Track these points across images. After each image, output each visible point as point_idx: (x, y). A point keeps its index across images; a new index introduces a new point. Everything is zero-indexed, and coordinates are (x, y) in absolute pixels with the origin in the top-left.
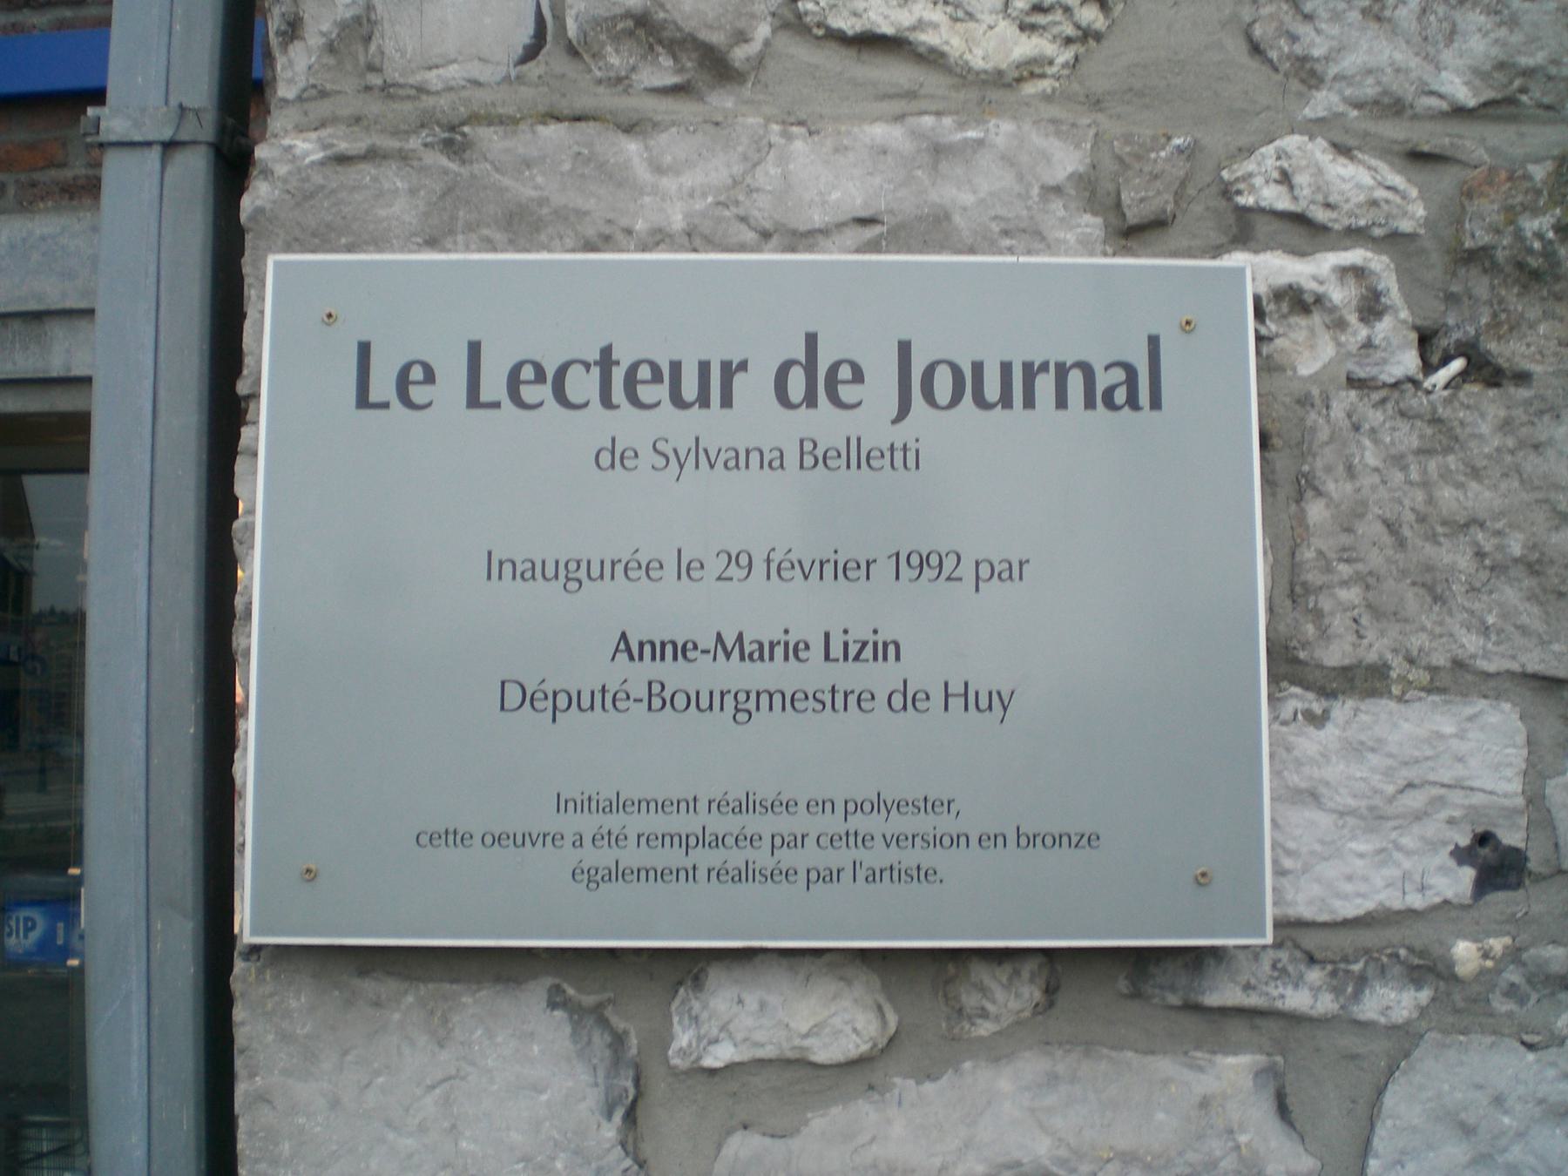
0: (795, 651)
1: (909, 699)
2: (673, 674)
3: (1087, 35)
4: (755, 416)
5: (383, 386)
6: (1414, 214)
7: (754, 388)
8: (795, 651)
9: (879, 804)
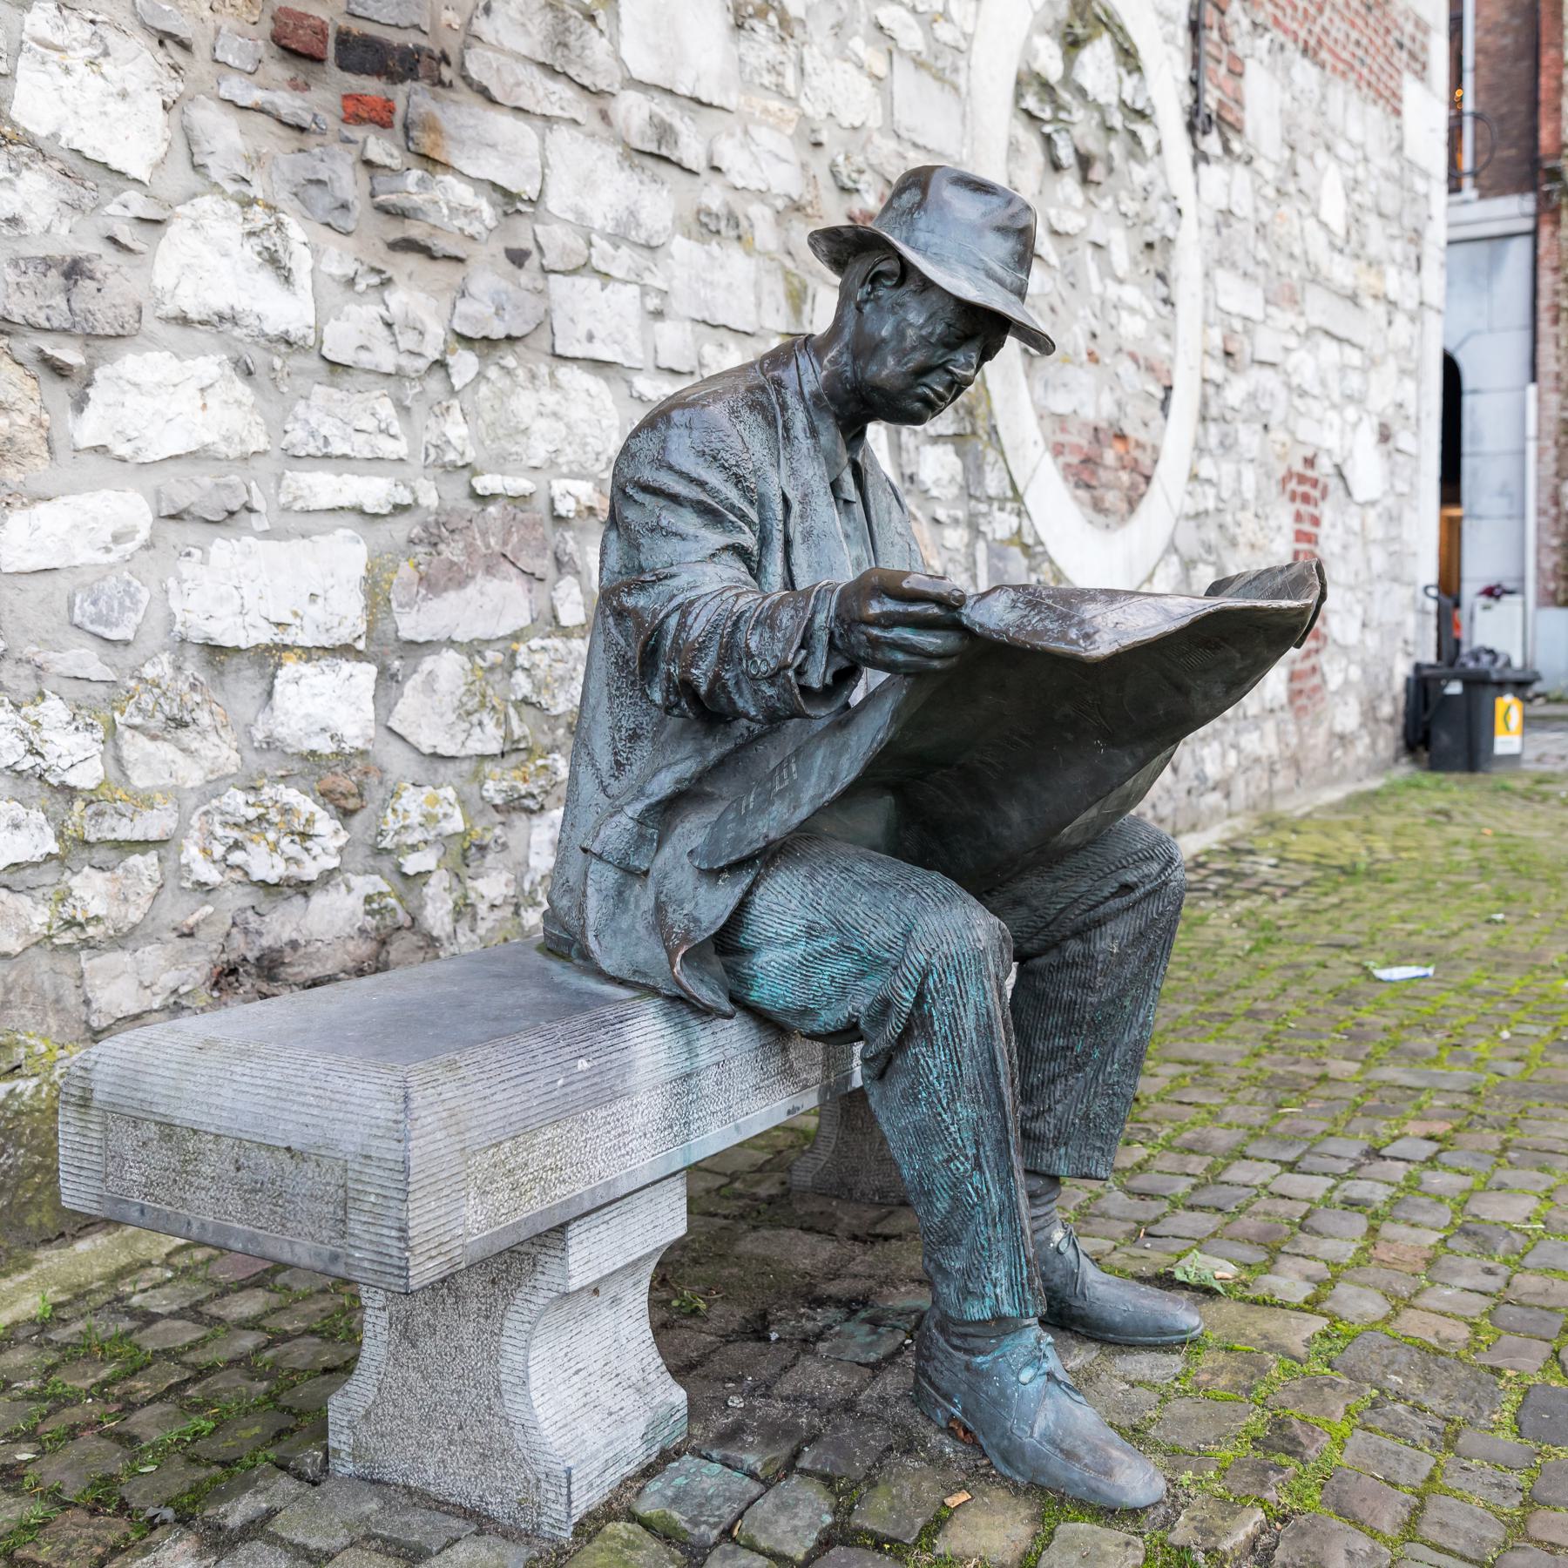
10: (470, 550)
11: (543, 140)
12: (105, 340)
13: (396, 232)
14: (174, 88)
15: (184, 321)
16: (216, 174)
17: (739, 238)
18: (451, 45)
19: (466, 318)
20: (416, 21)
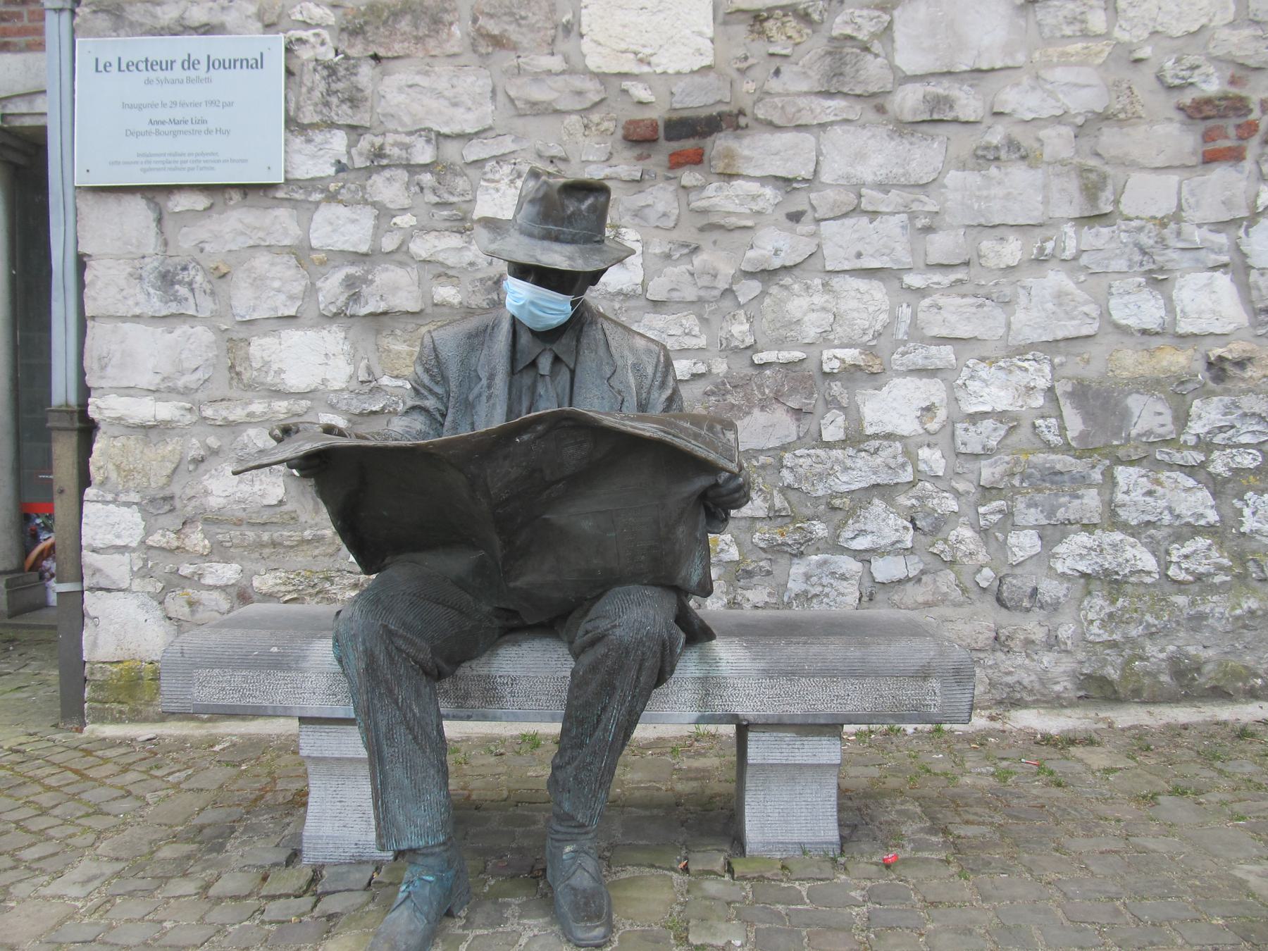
0: (186, 122)
1: (209, 132)
2: (161, 128)
4: (177, 72)
5: (101, 67)
6: (332, 20)
7: (177, 66)
8: (186, 122)
9: (202, 154)
10: (748, 398)
11: (818, 139)
13: (703, 221)
17: (1023, 158)
18: (746, 104)
19: (749, 260)
20: (718, 98)
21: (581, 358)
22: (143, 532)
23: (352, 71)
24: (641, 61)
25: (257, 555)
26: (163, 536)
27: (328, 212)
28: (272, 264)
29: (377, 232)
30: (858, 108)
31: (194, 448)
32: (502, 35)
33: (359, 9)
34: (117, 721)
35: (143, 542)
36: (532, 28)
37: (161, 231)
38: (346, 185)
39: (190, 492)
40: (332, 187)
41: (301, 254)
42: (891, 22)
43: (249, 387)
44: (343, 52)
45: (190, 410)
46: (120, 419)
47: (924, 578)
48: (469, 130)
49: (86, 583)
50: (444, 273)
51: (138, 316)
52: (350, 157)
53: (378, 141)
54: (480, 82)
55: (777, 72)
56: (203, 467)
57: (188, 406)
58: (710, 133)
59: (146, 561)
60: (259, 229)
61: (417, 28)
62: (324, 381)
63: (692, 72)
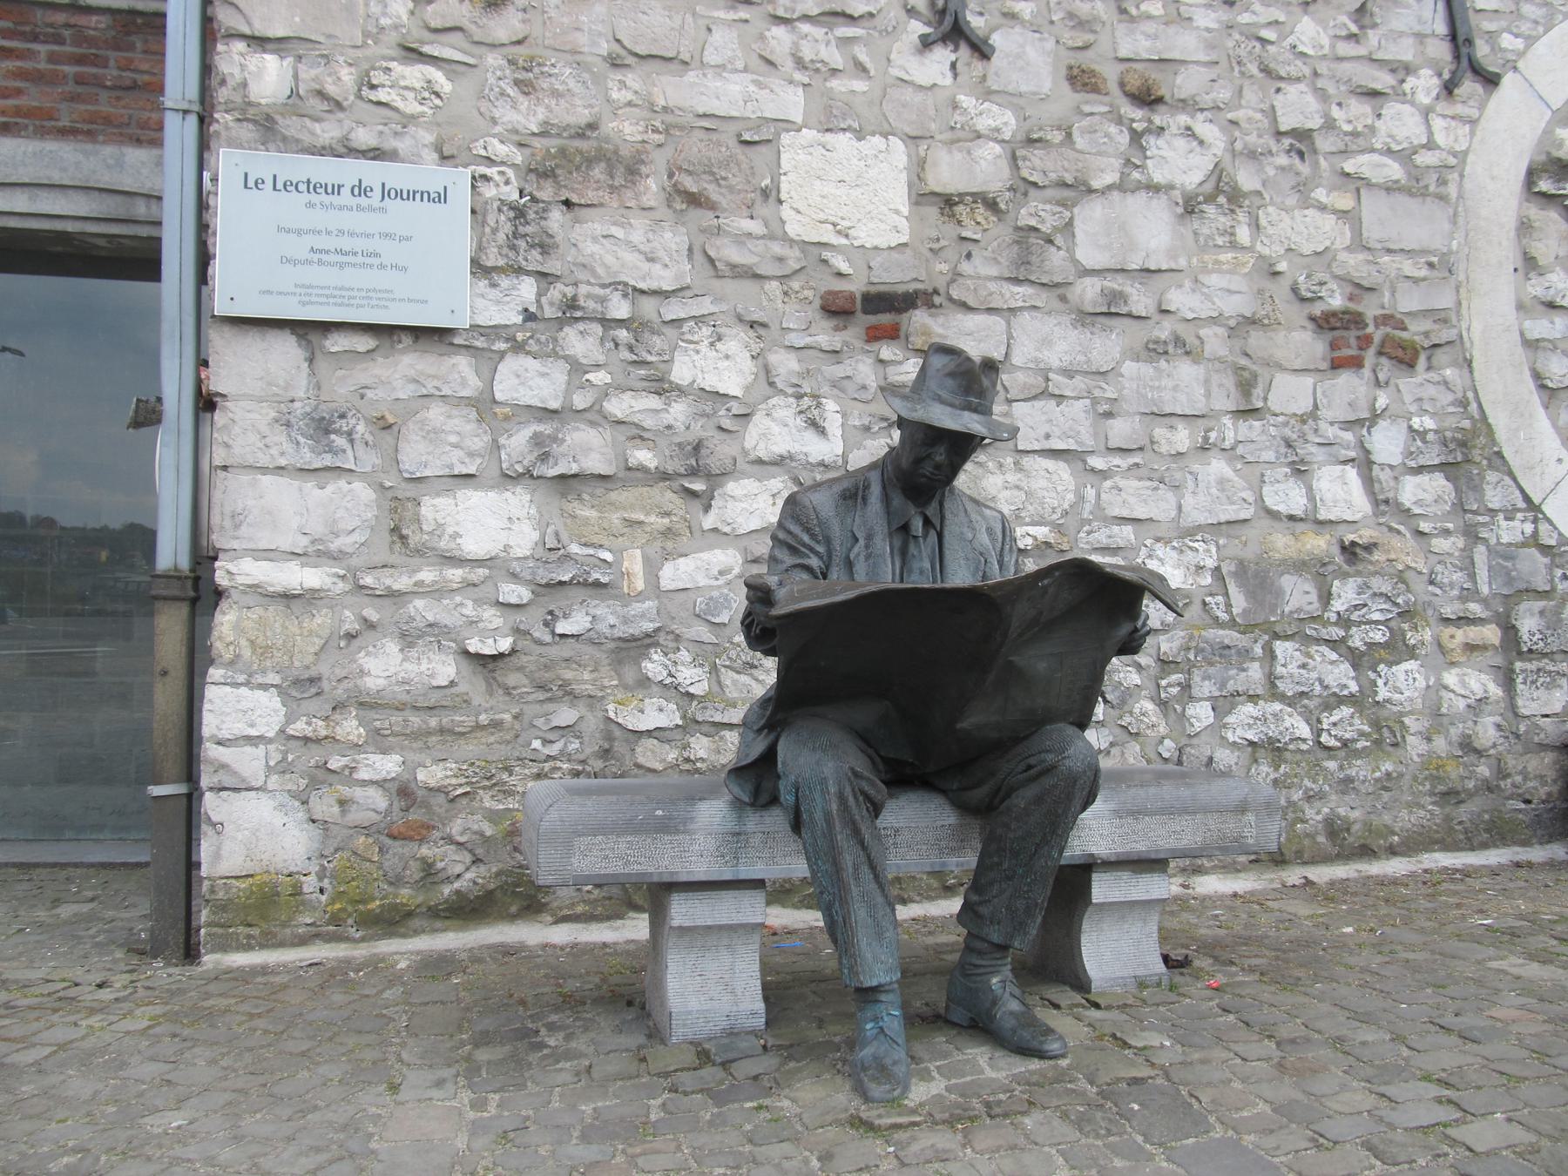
0: (355, 254)
1: (382, 266)
2: (324, 257)
3: (437, 107)
4: (346, 197)
5: (251, 183)
7: (346, 191)
8: (355, 254)
11: (1009, 324)
12: (716, 478)
14: (756, 347)
15: (760, 462)
16: (780, 385)
17: (1187, 353)
18: (941, 283)
21: (947, 522)
22: (283, 719)
23: (543, 215)
24: (839, 232)
25: (420, 744)
26: (309, 723)
27: (510, 367)
28: (449, 417)
29: (568, 393)
30: (1044, 296)
31: (350, 623)
32: (700, 194)
33: (548, 150)
34: (248, 948)
35: (282, 731)
36: (731, 189)
37: (313, 373)
38: (535, 333)
39: (340, 673)
40: (520, 337)
41: (484, 406)
42: (1071, 219)
43: (419, 552)
44: (530, 194)
45: (343, 577)
46: (256, 586)
47: (1113, 751)
48: (665, 288)
49: (205, 782)
50: (639, 435)
51: (282, 468)
52: (540, 306)
53: (570, 291)
54: (677, 239)
55: (969, 256)
56: (356, 643)
57: (342, 572)
58: (906, 310)
59: (285, 753)
60: (434, 377)
61: (612, 177)
62: (507, 548)
63: (890, 248)
